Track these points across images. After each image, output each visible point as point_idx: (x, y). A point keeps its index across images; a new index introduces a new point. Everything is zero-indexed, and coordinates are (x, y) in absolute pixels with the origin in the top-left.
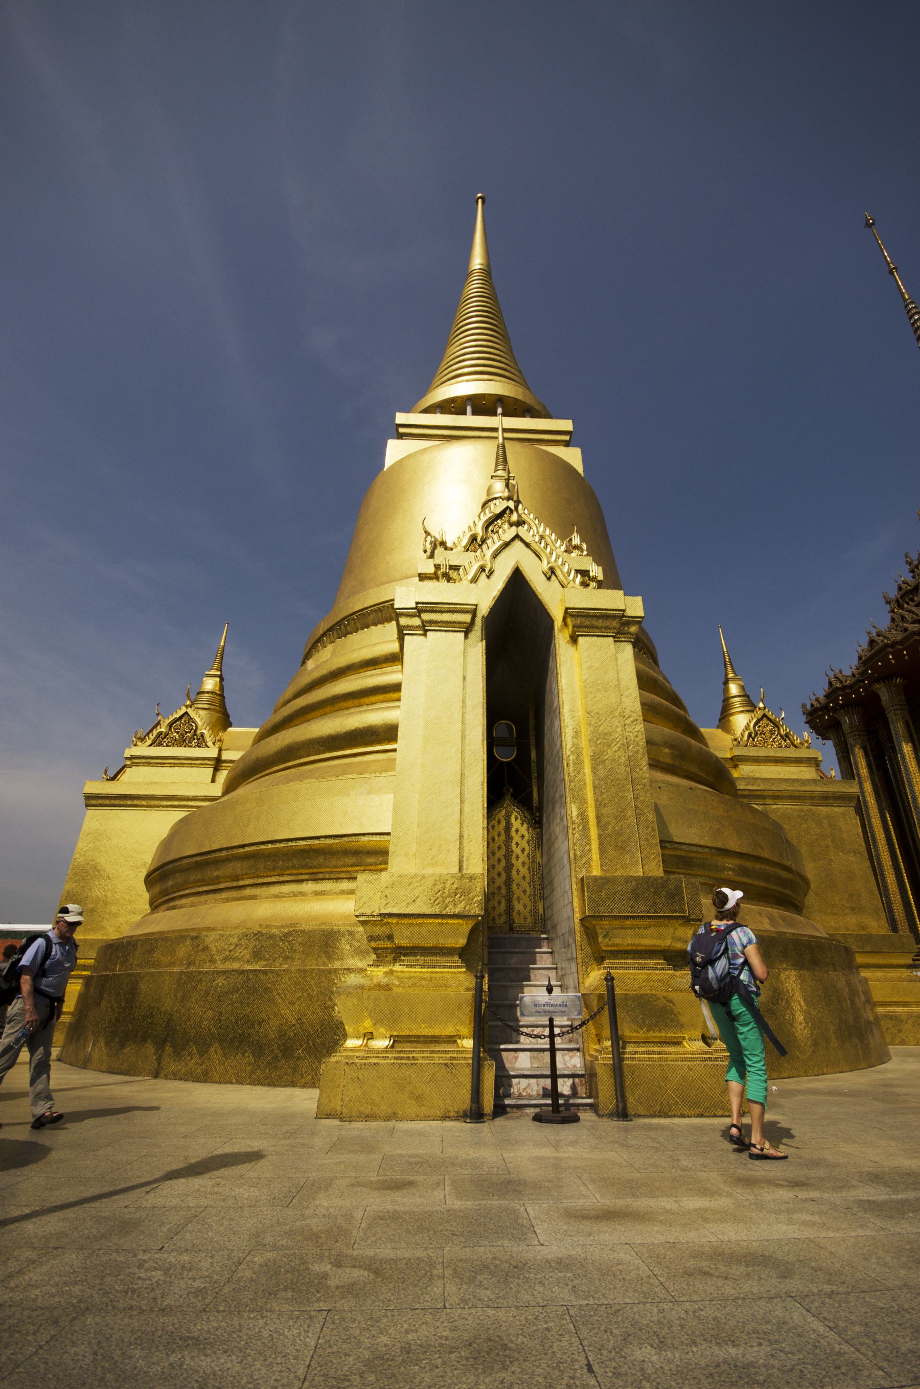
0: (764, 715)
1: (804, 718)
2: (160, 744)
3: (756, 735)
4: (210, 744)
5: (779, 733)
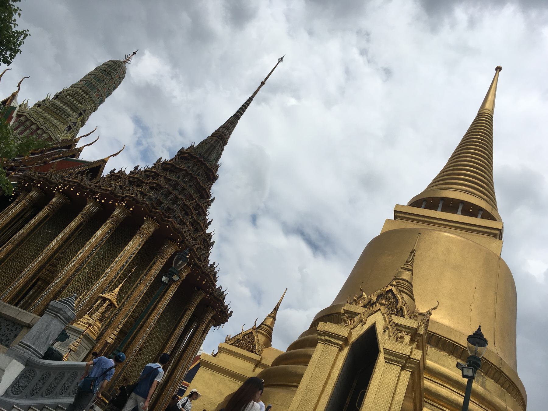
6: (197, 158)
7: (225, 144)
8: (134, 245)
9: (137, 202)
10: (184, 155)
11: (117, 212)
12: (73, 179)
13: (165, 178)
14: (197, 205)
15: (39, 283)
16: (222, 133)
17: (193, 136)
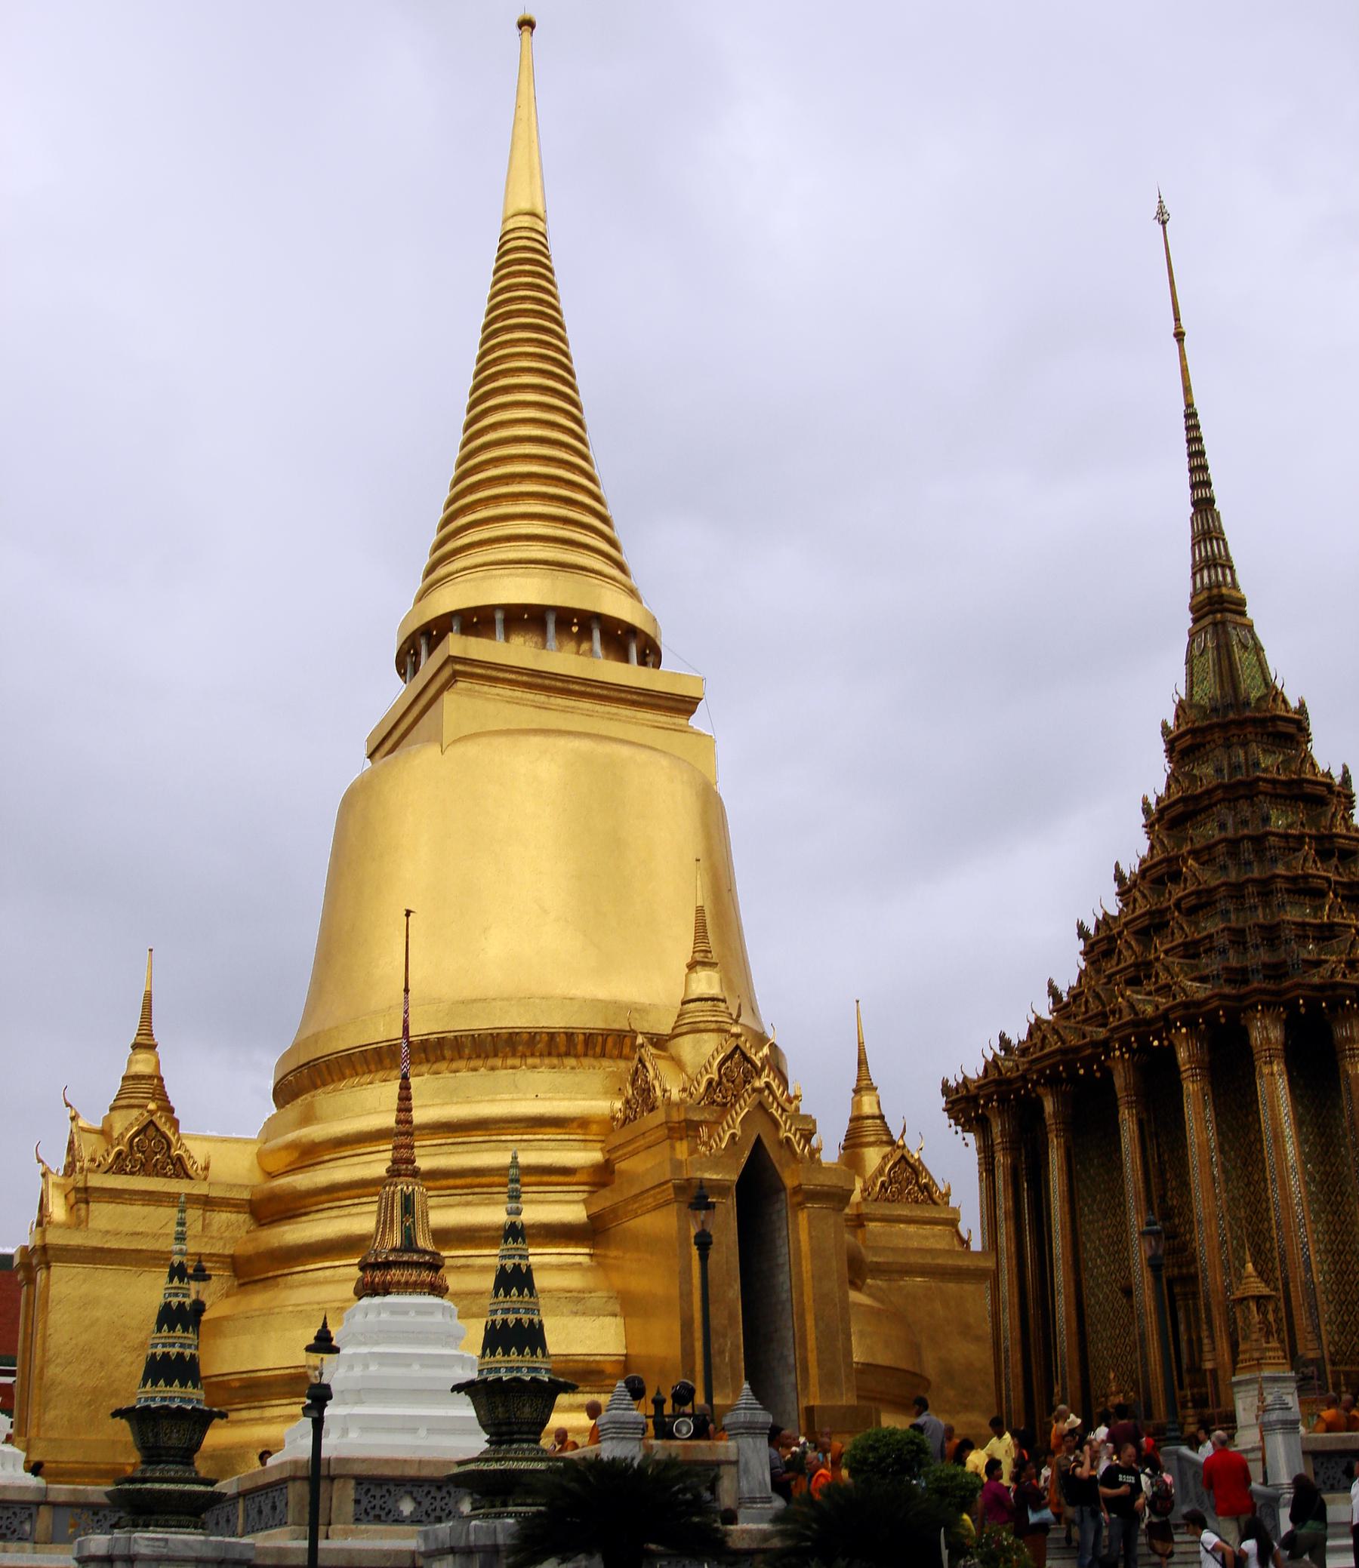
0: (903, 1157)
1: (942, 1101)
2: (121, 1171)
3: (891, 1183)
4: (191, 1172)
5: (917, 1182)
6: (1218, 725)
7: (1238, 606)
8: (1276, 1089)
9: (1199, 1004)
10: (1185, 744)
11: (1182, 1054)
12: (1042, 1049)
13: (1195, 854)
14: (1319, 839)
15: (1177, 1290)
16: (1210, 589)
17: (1159, 683)
